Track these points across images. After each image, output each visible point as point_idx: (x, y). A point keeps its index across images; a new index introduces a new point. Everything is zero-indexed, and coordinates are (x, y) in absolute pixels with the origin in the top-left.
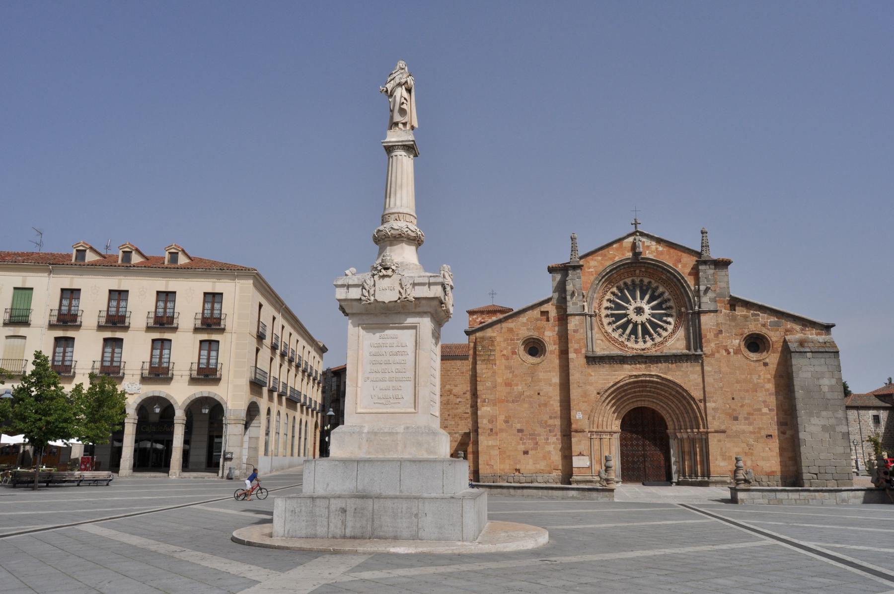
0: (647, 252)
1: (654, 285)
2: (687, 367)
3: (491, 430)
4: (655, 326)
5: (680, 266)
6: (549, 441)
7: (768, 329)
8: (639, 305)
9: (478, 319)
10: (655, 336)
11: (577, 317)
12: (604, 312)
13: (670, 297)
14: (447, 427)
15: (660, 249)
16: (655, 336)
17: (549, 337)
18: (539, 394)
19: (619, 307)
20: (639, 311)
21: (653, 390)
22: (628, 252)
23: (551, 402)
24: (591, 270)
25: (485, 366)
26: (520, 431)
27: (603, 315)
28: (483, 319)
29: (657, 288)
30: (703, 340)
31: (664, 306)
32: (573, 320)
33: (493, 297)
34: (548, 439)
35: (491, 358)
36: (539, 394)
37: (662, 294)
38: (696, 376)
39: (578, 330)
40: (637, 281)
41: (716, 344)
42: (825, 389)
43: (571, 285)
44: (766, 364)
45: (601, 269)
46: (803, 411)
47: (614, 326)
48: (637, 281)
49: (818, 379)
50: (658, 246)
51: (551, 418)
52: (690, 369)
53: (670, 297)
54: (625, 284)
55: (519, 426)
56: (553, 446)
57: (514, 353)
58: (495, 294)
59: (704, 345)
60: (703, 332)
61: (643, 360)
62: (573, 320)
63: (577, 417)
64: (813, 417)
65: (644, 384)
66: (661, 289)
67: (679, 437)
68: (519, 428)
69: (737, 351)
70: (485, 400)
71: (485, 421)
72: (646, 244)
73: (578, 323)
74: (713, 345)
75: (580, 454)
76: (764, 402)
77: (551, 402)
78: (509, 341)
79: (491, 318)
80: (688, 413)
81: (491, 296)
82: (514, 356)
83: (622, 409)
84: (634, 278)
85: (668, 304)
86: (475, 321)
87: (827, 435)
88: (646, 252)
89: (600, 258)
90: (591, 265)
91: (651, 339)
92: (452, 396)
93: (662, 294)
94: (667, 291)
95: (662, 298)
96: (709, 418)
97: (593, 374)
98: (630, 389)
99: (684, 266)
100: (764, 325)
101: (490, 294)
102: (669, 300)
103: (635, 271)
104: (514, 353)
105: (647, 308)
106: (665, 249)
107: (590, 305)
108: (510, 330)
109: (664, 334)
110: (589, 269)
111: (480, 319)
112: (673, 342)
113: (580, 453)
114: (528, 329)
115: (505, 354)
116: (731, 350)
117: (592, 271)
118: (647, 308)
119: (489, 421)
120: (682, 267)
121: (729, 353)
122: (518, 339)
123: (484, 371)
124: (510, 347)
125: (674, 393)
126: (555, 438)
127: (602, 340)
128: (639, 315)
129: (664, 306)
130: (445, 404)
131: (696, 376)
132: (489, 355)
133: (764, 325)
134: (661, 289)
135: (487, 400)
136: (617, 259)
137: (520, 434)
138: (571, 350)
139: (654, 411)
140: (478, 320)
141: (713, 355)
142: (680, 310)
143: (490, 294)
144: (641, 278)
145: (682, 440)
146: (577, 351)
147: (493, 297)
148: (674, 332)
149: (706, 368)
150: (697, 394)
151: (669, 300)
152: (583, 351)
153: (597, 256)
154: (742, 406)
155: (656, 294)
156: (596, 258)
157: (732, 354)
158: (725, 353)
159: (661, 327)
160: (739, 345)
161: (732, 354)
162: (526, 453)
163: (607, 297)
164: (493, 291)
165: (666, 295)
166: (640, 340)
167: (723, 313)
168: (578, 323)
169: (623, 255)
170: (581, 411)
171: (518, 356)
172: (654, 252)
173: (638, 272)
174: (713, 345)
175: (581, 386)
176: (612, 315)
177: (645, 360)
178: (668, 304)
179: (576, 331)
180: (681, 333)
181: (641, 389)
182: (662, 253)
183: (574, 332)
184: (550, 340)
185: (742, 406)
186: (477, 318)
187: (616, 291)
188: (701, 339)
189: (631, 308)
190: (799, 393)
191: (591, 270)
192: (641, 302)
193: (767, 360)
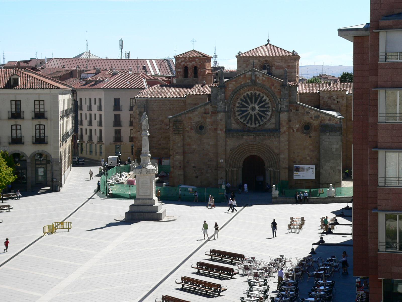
0: (258, 80)
1: (262, 96)
2: (273, 138)
3: (180, 167)
4: (261, 116)
5: (273, 88)
6: (208, 172)
7: (313, 120)
8: (254, 106)
9: (182, 63)
10: (261, 121)
11: (222, 113)
12: (237, 109)
13: (269, 102)
14: (160, 145)
15: (264, 79)
16: (261, 121)
17: (209, 122)
18: (203, 150)
19: (244, 106)
20: (253, 109)
21: (257, 148)
22: (248, 80)
23: (209, 154)
24: (229, 89)
25: (177, 136)
26: (194, 167)
27: (236, 110)
28: (186, 63)
29: (263, 97)
30: (281, 126)
31: (266, 106)
32: (220, 115)
33: (193, 44)
34: (207, 171)
35: (180, 132)
36: (203, 150)
37: (265, 100)
38: (276, 143)
39: (222, 119)
40: (253, 92)
41: (286, 128)
42: (334, 150)
43: (220, 97)
44: (310, 137)
45: (234, 88)
46: (323, 160)
47: (241, 116)
48: (253, 92)
49: (331, 145)
50: (263, 77)
51: (209, 161)
52: (274, 139)
53: (269, 102)
54: (247, 94)
55: (193, 165)
56: (210, 174)
57: (192, 129)
58: (195, 41)
59: (281, 128)
60: (281, 122)
61: (252, 135)
62: (220, 115)
63: (221, 161)
64: (327, 162)
65: (253, 146)
66: (265, 98)
67: (270, 170)
68: (194, 166)
69: (297, 130)
70: (177, 152)
71: (177, 163)
72: (257, 76)
73: (222, 116)
74: (285, 128)
75: (222, 178)
76: (308, 154)
77: (209, 154)
78: (189, 124)
79: (192, 63)
80: (273, 159)
81: (192, 42)
82: (192, 131)
83: (243, 156)
84: (252, 92)
85: (268, 105)
86: (180, 64)
87: (332, 171)
88: (257, 80)
89: (234, 83)
90: (230, 86)
91: (258, 123)
92: (163, 124)
93: (265, 100)
94: (267, 99)
95: (265, 102)
96: (281, 162)
97: (229, 141)
98: (247, 147)
99: (275, 88)
100: (311, 118)
101: (191, 41)
102: (268, 103)
103: (252, 88)
104: (192, 129)
105: (257, 107)
106: (266, 79)
107: (228, 107)
108: (190, 118)
109: (265, 120)
110: (229, 88)
111: (183, 63)
112: (268, 125)
113: (222, 178)
114: (198, 118)
115: (187, 130)
116: (295, 130)
117: (230, 90)
118: (257, 107)
119: (179, 163)
120: (274, 88)
121: (294, 131)
122: (194, 123)
123: (176, 139)
124: (190, 127)
125: (267, 150)
126: (211, 170)
127: (234, 123)
128: (253, 111)
129: (266, 106)
130: (159, 130)
131: (276, 143)
132: (179, 131)
133: (311, 118)
134: (265, 98)
135: (178, 153)
136: (242, 83)
137: (194, 168)
138: (219, 129)
139: (259, 157)
140: (182, 64)
141: (285, 133)
142: (273, 109)
143: (191, 41)
144: (255, 92)
145: (270, 171)
146: (221, 130)
147: (193, 44)
148: (269, 120)
149: (282, 139)
150: (277, 151)
151: (268, 103)
152: (224, 130)
153: (233, 81)
154: (298, 156)
155: (262, 100)
156: (232, 83)
157: (295, 131)
158: (292, 131)
159: (264, 117)
160: (299, 127)
161: (295, 131)
162: (197, 177)
163: (238, 101)
164: (193, 39)
165: (267, 101)
166: (253, 123)
167: (292, 111)
168: (222, 116)
169: (246, 81)
170: (222, 158)
171: (193, 131)
172: (261, 80)
173: (253, 89)
174: (285, 128)
175: (223, 147)
176: (241, 111)
177: (253, 135)
178: (268, 105)
179: (221, 120)
180: (273, 120)
181: (252, 148)
182: (264, 81)
183: (220, 121)
184: (209, 123)
185: (298, 156)
186: (181, 62)
187: (243, 98)
188: (280, 125)
189: (250, 107)
190: (322, 151)
191: (229, 89)
192: (255, 104)
193: (311, 135)
